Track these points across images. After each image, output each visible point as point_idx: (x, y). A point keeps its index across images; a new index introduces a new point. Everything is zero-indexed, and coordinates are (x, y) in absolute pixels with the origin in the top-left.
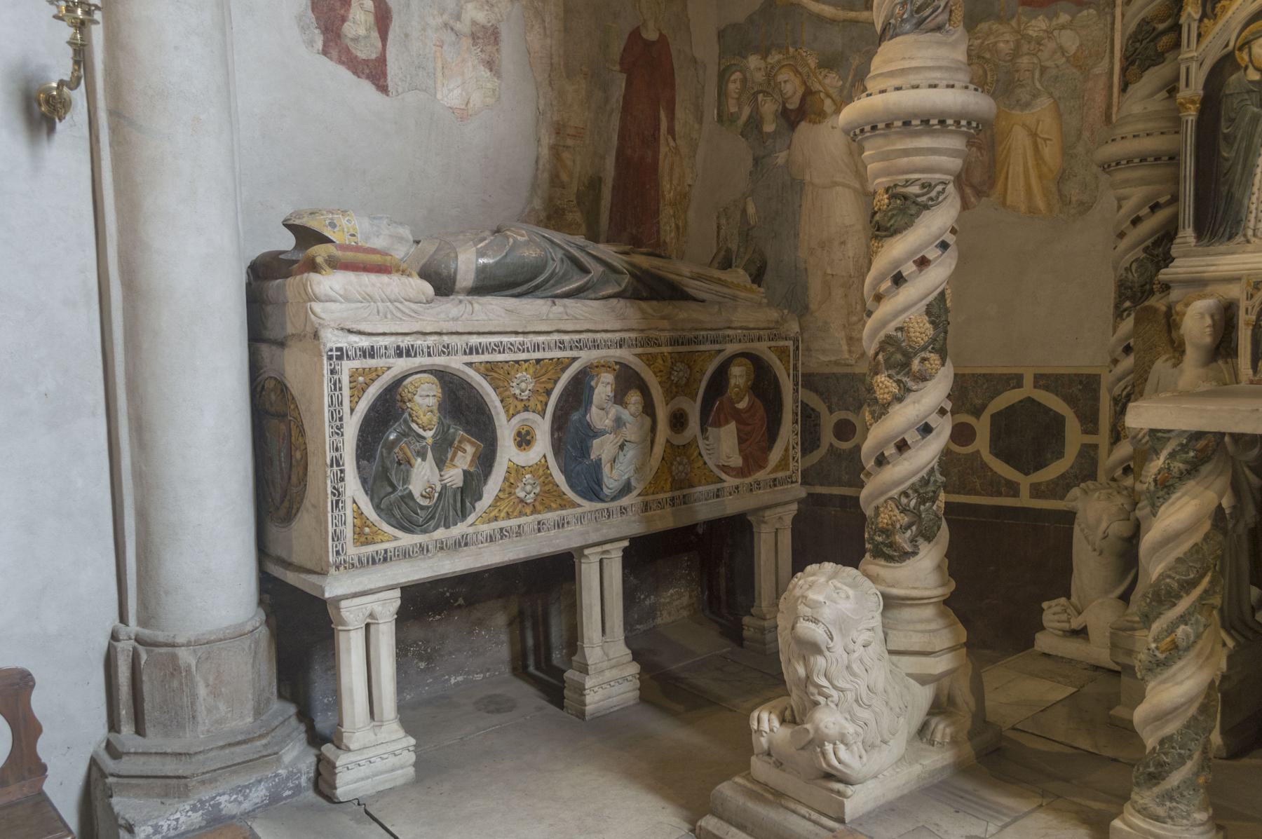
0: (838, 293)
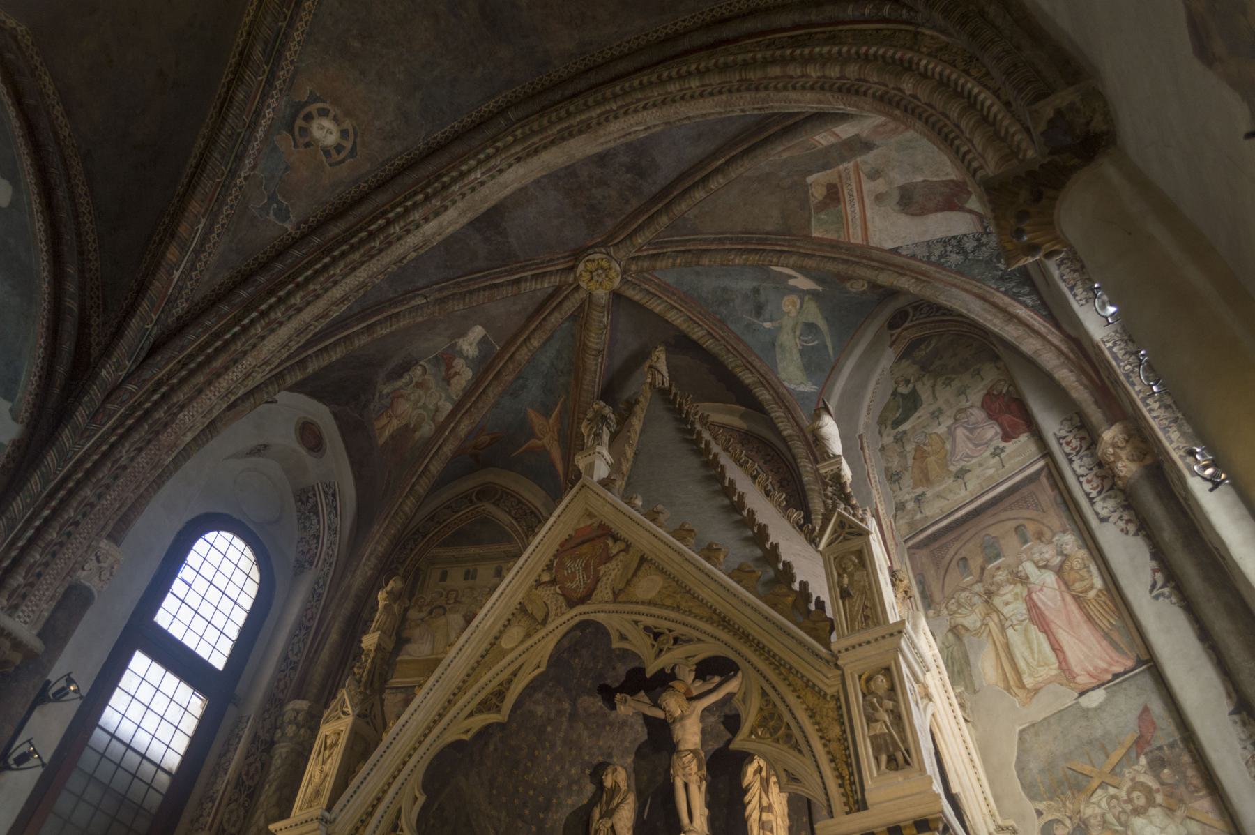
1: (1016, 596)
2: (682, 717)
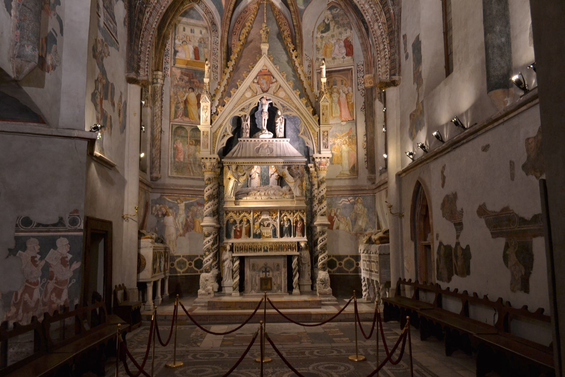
0: (171, 243)
2: (265, 104)
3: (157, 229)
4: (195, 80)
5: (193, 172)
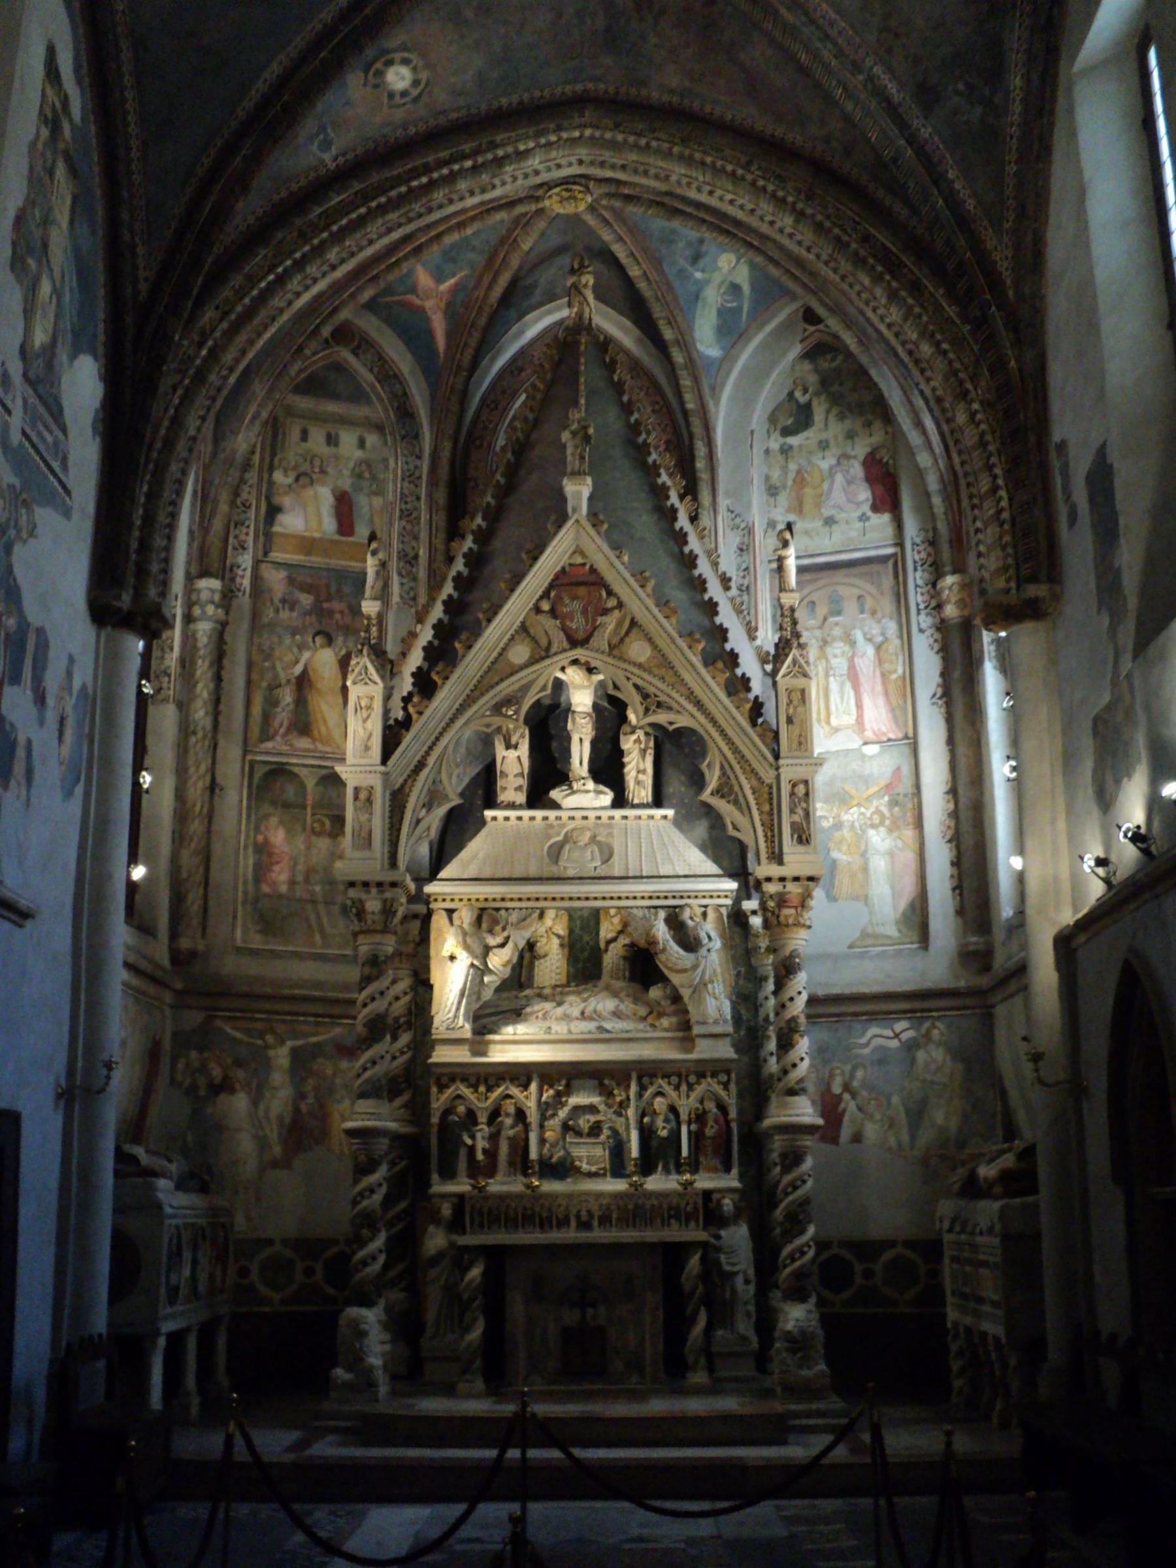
1: (843, 653)
3: (189, 1138)
4: (336, 605)
5: (322, 931)
